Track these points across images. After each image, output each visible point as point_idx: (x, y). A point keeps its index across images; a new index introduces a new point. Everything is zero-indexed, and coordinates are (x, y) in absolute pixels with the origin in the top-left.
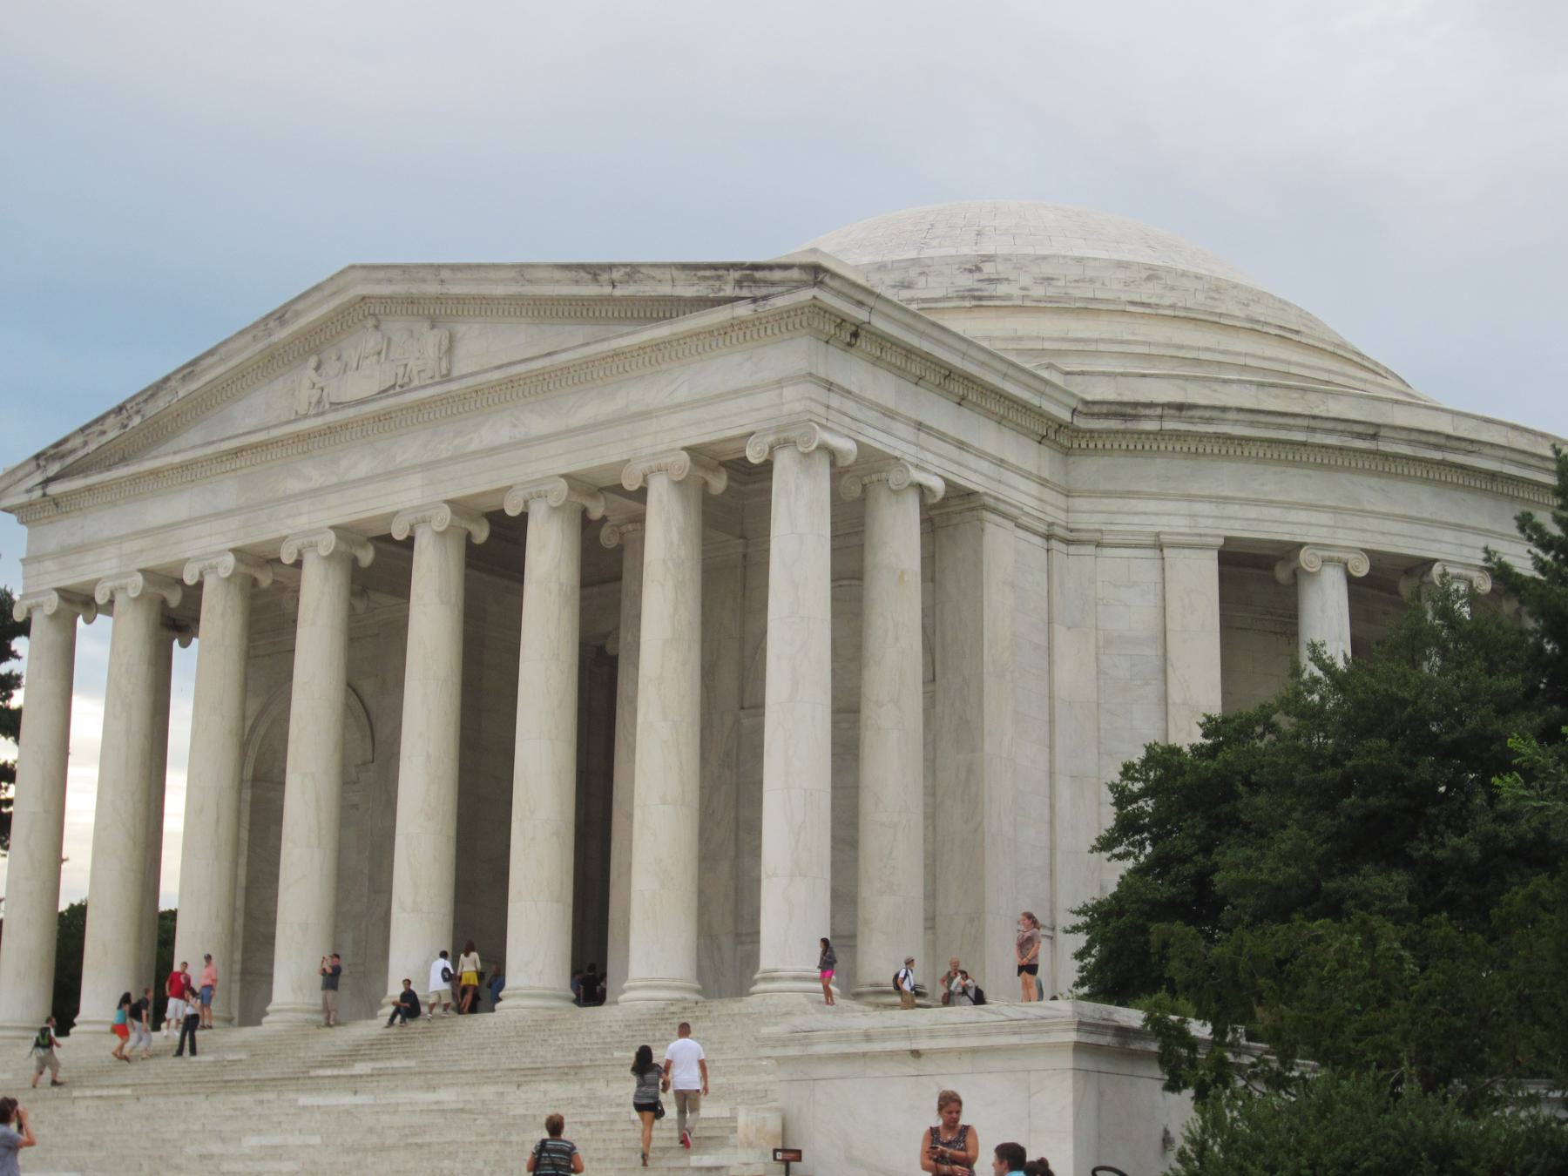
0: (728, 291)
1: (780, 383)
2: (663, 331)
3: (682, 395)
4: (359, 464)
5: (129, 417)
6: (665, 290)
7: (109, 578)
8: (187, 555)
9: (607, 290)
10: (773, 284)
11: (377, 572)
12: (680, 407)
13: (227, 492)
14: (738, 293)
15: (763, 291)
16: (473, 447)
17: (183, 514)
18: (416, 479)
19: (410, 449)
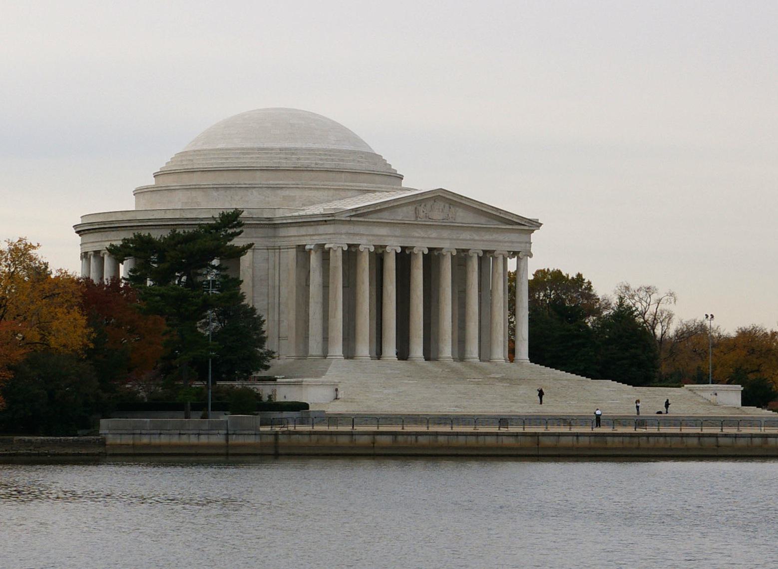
0: (523, 223)
1: (526, 242)
2: (511, 227)
3: (507, 239)
4: (434, 234)
5: (377, 206)
6: (510, 218)
7: (364, 245)
8: (387, 244)
9: (498, 214)
10: (532, 224)
11: (432, 258)
12: (505, 242)
13: (398, 231)
14: (526, 224)
15: (530, 225)
16: (461, 238)
17: (385, 233)
18: (448, 241)
19: (445, 234)
